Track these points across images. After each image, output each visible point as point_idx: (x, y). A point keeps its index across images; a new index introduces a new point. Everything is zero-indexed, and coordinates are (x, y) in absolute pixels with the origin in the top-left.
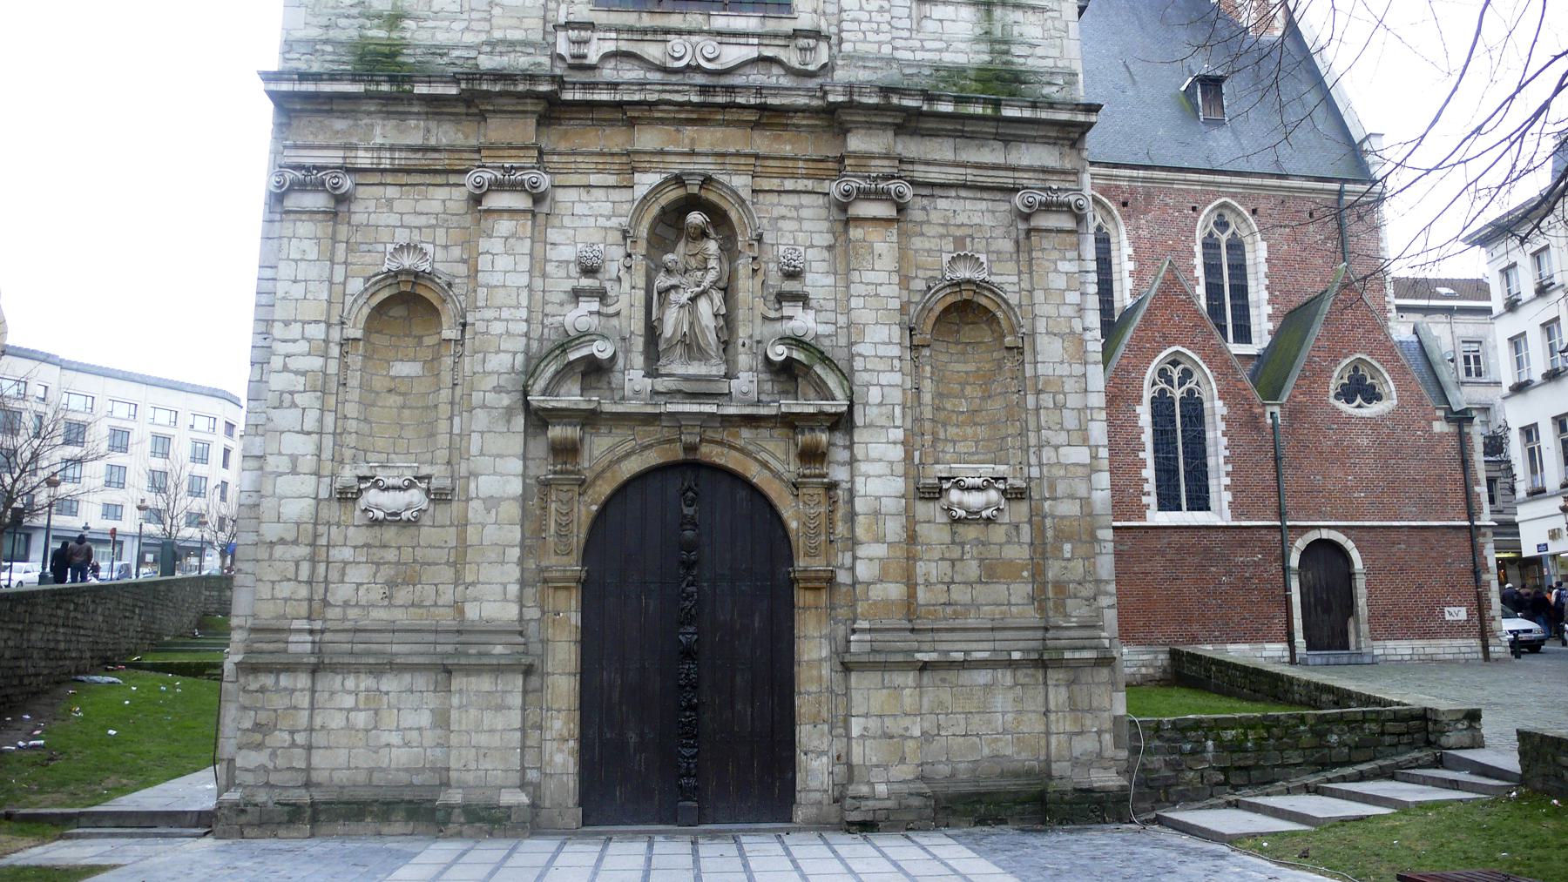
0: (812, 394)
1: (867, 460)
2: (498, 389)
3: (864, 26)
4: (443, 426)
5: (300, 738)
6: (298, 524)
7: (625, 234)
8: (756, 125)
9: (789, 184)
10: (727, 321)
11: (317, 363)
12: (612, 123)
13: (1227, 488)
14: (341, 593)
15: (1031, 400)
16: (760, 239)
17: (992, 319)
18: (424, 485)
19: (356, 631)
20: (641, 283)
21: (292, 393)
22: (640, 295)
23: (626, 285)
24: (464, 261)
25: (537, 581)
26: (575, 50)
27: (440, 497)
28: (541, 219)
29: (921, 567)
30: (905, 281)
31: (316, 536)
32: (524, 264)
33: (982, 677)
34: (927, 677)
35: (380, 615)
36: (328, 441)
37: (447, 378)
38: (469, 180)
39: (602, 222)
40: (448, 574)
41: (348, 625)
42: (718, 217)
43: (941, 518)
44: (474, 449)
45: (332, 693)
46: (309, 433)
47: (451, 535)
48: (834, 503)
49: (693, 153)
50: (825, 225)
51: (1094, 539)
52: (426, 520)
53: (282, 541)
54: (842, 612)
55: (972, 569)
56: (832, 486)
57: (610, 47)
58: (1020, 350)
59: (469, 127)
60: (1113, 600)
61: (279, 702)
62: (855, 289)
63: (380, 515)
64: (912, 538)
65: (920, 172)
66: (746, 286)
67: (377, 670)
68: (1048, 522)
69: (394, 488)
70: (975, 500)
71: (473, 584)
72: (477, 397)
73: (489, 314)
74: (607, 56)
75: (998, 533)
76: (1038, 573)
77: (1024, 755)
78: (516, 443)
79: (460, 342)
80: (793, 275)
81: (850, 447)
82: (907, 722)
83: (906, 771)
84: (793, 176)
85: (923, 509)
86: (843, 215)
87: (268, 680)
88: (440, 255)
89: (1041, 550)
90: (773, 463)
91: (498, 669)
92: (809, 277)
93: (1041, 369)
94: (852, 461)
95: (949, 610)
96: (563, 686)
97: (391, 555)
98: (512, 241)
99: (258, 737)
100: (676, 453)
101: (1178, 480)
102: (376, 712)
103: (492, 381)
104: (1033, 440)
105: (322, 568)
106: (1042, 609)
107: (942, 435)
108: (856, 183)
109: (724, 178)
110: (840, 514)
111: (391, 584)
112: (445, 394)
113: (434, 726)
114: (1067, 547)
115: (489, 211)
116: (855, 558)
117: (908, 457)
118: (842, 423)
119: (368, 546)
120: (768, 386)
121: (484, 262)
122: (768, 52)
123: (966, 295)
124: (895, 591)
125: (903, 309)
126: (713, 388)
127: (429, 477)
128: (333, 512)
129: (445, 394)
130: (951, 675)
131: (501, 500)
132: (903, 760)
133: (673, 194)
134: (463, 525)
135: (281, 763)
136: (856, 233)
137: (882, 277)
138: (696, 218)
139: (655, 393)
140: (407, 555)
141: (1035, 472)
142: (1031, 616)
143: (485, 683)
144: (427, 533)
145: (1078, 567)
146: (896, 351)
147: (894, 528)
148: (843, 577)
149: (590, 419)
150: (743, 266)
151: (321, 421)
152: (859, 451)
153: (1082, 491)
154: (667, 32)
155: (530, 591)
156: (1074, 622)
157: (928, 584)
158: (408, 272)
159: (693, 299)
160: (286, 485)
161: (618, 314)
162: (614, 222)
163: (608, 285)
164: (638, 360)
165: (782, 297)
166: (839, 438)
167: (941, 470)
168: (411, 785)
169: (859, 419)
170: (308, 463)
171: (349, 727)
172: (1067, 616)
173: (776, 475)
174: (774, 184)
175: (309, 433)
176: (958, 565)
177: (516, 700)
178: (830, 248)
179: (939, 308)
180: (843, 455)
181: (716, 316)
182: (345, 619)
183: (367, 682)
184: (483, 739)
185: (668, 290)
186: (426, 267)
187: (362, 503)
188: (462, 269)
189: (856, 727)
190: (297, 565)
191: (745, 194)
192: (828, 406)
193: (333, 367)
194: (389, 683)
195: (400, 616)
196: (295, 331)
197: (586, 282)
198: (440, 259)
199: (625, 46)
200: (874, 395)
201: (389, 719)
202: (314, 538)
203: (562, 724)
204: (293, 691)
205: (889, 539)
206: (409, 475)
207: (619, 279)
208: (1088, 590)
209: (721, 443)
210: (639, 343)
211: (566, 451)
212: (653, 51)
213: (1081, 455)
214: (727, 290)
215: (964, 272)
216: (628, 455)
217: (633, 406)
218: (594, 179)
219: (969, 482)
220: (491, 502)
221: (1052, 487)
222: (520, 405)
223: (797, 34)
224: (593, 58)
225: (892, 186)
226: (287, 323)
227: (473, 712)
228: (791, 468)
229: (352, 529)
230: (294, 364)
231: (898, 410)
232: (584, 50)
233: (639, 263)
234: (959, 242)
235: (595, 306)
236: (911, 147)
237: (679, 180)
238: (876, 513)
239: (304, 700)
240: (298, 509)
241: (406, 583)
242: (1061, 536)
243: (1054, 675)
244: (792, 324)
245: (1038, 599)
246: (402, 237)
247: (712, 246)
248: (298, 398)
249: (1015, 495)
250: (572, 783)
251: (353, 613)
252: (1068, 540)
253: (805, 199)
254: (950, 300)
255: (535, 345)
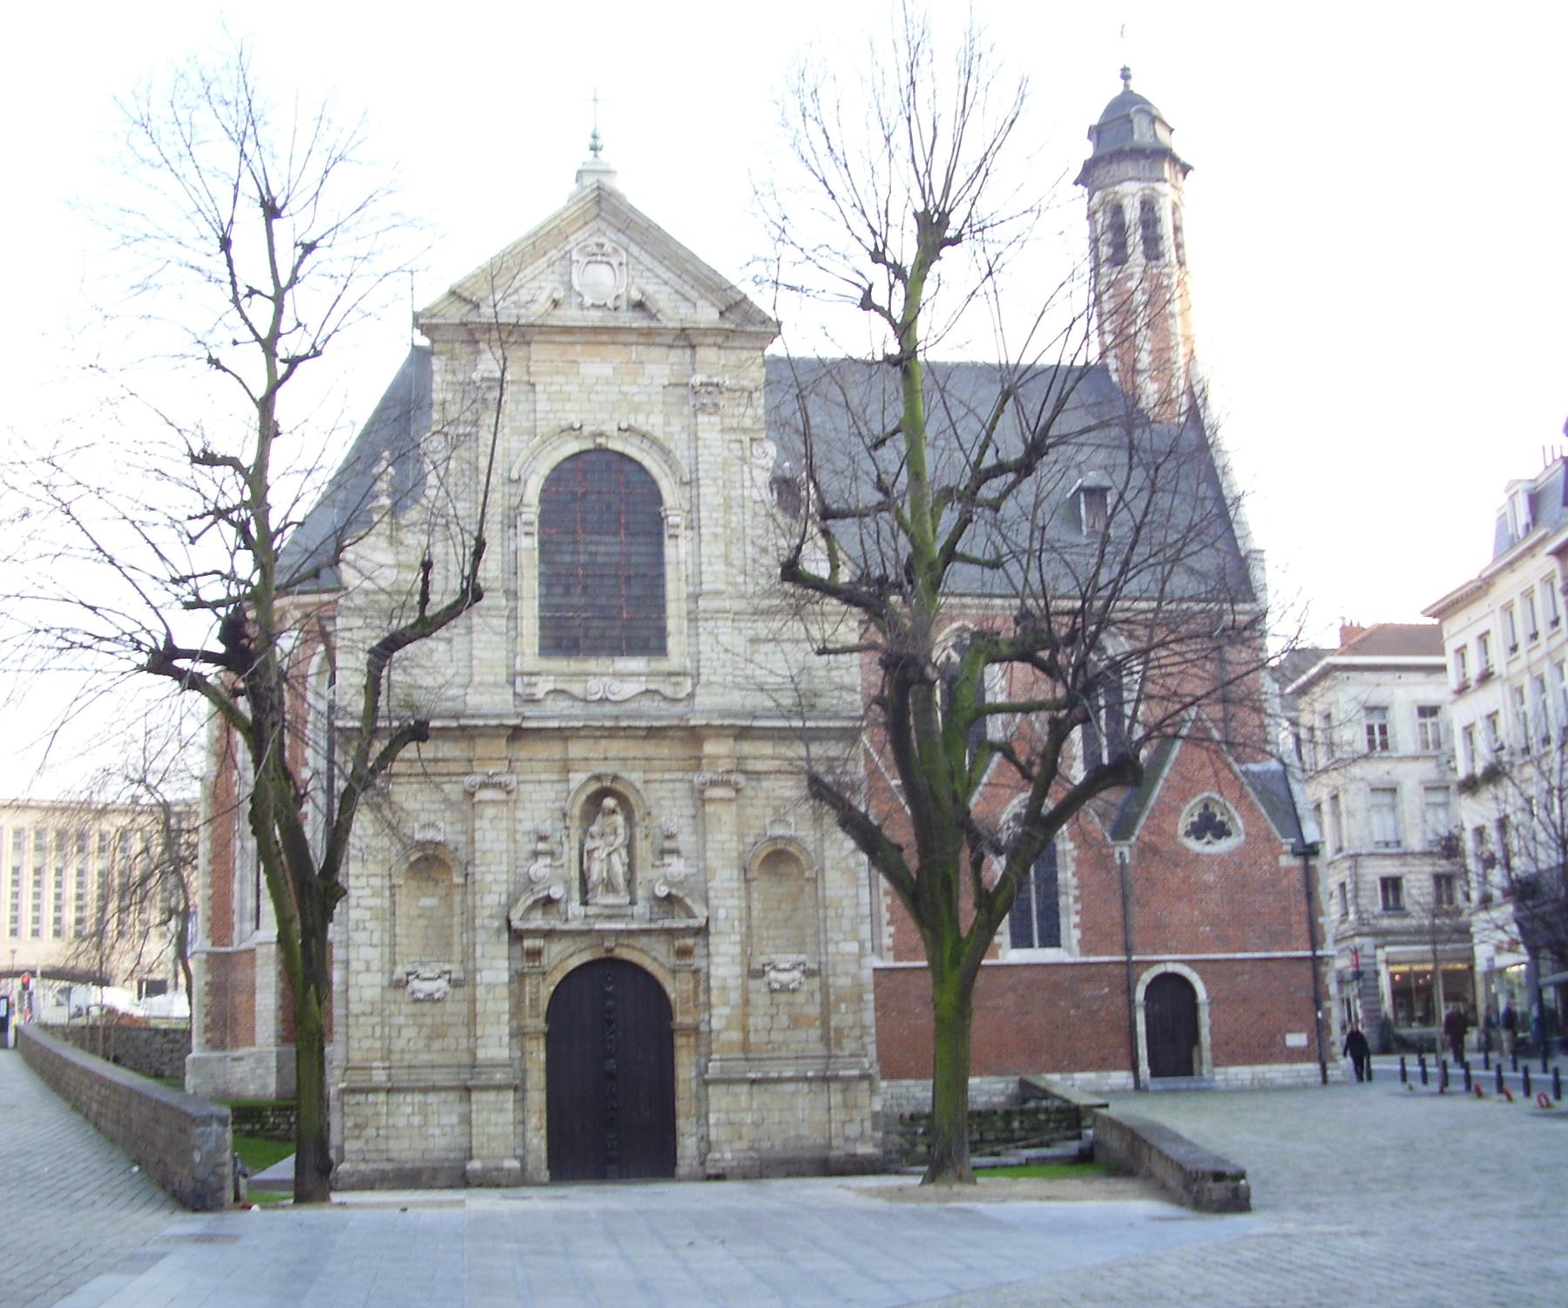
0: (683, 915)
1: (717, 953)
2: (491, 917)
3: (715, 664)
4: (456, 939)
5: (382, 1132)
6: (373, 1004)
7: (565, 815)
8: (645, 738)
9: (667, 776)
10: (631, 867)
11: (377, 902)
12: (553, 738)
13: (1076, 926)
14: (399, 1044)
15: (821, 912)
16: (649, 814)
17: (796, 860)
18: (447, 976)
19: (410, 1067)
20: (576, 845)
21: (364, 921)
22: (575, 853)
23: (566, 847)
24: (466, 832)
25: (519, 1034)
26: (528, 691)
27: (455, 984)
28: (511, 805)
29: (751, 1021)
30: (741, 837)
31: (383, 1010)
32: (504, 836)
33: (790, 1087)
34: (755, 1088)
35: (424, 1057)
36: (387, 950)
37: (457, 908)
38: (467, 780)
39: (549, 805)
40: (463, 1031)
41: (406, 1064)
42: (623, 801)
43: (764, 989)
44: (478, 953)
45: (398, 1106)
46: (376, 946)
47: (464, 1008)
48: (697, 982)
49: (606, 759)
50: (690, 802)
51: (860, 999)
52: (449, 997)
53: (363, 1014)
54: (703, 1049)
55: (784, 1021)
56: (696, 972)
57: (551, 686)
58: (815, 880)
59: (464, 745)
60: (873, 1038)
61: (369, 1111)
62: (709, 845)
63: (421, 996)
64: (747, 1002)
65: (752, 765)
66: (642, 847)
67: (425, 1090)
68: (831, 990)
69: (429, 979)
70: (785, 977)
71: (481, 1037)
72: (478, 922)
73: (483, 869)
74: (548, 693)
75: (800, 998)
76: (825, 1023)
77: (816, 1135)
78: (504, 949)
79: (465, 885)
80: (670, 837)
81: (707, 945)
82: (743, 1115)
83: (744, 1144)
84: (669, 770)
85: (755, 984)
86: (700, 798)
87: (361, 1098)
88: (449, 829)
89: (826, 1008)
90: (660, 958)
91: (499, 1088)
92: (680, 838)
93: (828, 893)
94: (708, 955)
95: (770, 1047)
96: (537, 1097)
97: (428, 1020)
98: (495, 821)
99: (357, 1132)
100: (601, 954)
101: (1030, 919)
102: (426, 1116)
103: (487, 912)
104: (822, 937)
105: (387, 1029)
106: (828, 1045)
107: (765, 935)
108: (708, 776)
109: (624, 775)
110: (702, 987)
111: (430, 1038)
112: (456, 920)
113: (460, 1123)
114: (843, 1007)
115: (480, 802)
116: (710, 1016)
117: (744, 952)
118: (703, 932)
119: (414, 1015)
120: (656, 909)
121: (478, 835)
122: (652, 687)
123: (780, 846)
124: (735, 1036)
125: (740, 856)
126: (623, 912)
127: (449, 972)
128: (390, 995)
129: (456, 920)
130: (771, 1087)
131: (496, 986)
132: (740, 1138)
133: (594, 787)
134: (473, 1001)
135: (371, 1146)
136: (709, 808)
137: (726, 837)
138: (609, 802)
139: (586, 916)
140: (438, 1020)
141: (823, 959)
142: (820, 1049)
143: (491, 1096)
144: (449, 1007)
145: (850, 1019)
146: (736, 885)
147: (735, 997)
148: (704, 1028)
149: (549, 934)
150: (639, 833)
151: (382, 938)
152: (712, 949)
153: (853, 968)
154: (588, 674)
155: (514, 1041)
156: (846, 1053)
157: (756, 1030)
158: (430, 842)
159: (609, 855)
160: (364, 979)
161: (562, 866)
162: (557, 805)
163: (555, 847)
164: (576, 895)
165: (663, 852)
166: (700, 941)
167: (764, 959)
168: (447, 1159)
169: (712, 929)
170: (376, 965)
171: (409, 1125)
172: (842, 1048)
173: (662, 965)
174: (658, 776)
175: (376, 946)
176: (775, 1019)
177: (510, 1105)
178: (694, 817)
179: (764, 854)
180: (700, 951)
181: (623, 864)
182: (402, 1060)
183: (418, 1098)
184: (491, 1130)
185: (593, 850)
186: (440, 838)
187: (409, 989)
188: (463, 838)
189: (712, 1119)
190: (373, 1028)
191: (639, 785)
192: (694, 923)
193: (387, 903)
194: (432, 1098)
195: (437, 1058)
196: (363, 881)
197: (541, 846)
198: (445, 831)
199: (560, 686)
200: (722, 913)
201: (433, 1119)
202: (378, 1009)
203: (537, 1120)
204: (376, 1104)
205: (732, 1003)
206: (438, 971)
207: (561, 843)
208: (857, 1032)
209: (628, 946)
210: (576, 884)
211: (535, 954)
212: (576, 688)
213: (852, 947)
214: (630, 847)
215: (779, 831)
216: (571, 955)
217: (575, 925)
218: (543, 777)
219: (781, 966)
220: (491, 987)
221: (834, 968)
222: (505, 926)
223: (670, 674)
224: (540, 695)
225: (733, 778)
226: (358, 877)
227: (485, 1114)
228: (672, 961)
229: (403, 1006)
230: (364, 902)
231: (736, 923)
232: (534, 690)
233: (576, 833)
234: (776, 809)
235: (548, 861)
236: (747, 748)
237: (598, 778)
238: (724, 988)
239: (384, 1110)
240: (372, 993)
241: (438, 1037)
242: (839, 1000)
243: (834, 1086)
244: (670, 870)
245: (825, 1039)
246: (424, 818)
247: (619, 819)
248: (367, 925)
249: (809, 973)
250: (544, 1155)
251: (407, 1057)
252: (844, 1000)
253: (678, 785)
254: (770, 849)
255: (511, 888)
